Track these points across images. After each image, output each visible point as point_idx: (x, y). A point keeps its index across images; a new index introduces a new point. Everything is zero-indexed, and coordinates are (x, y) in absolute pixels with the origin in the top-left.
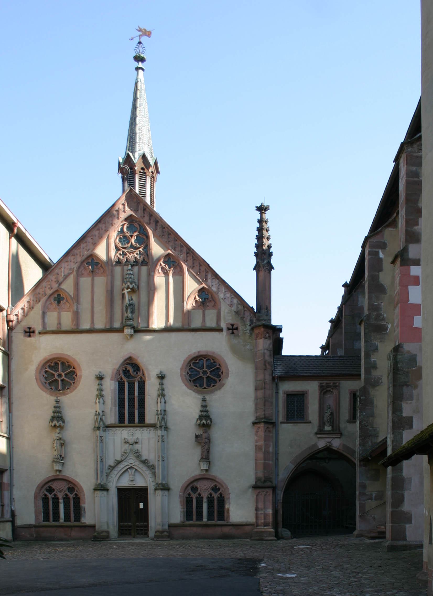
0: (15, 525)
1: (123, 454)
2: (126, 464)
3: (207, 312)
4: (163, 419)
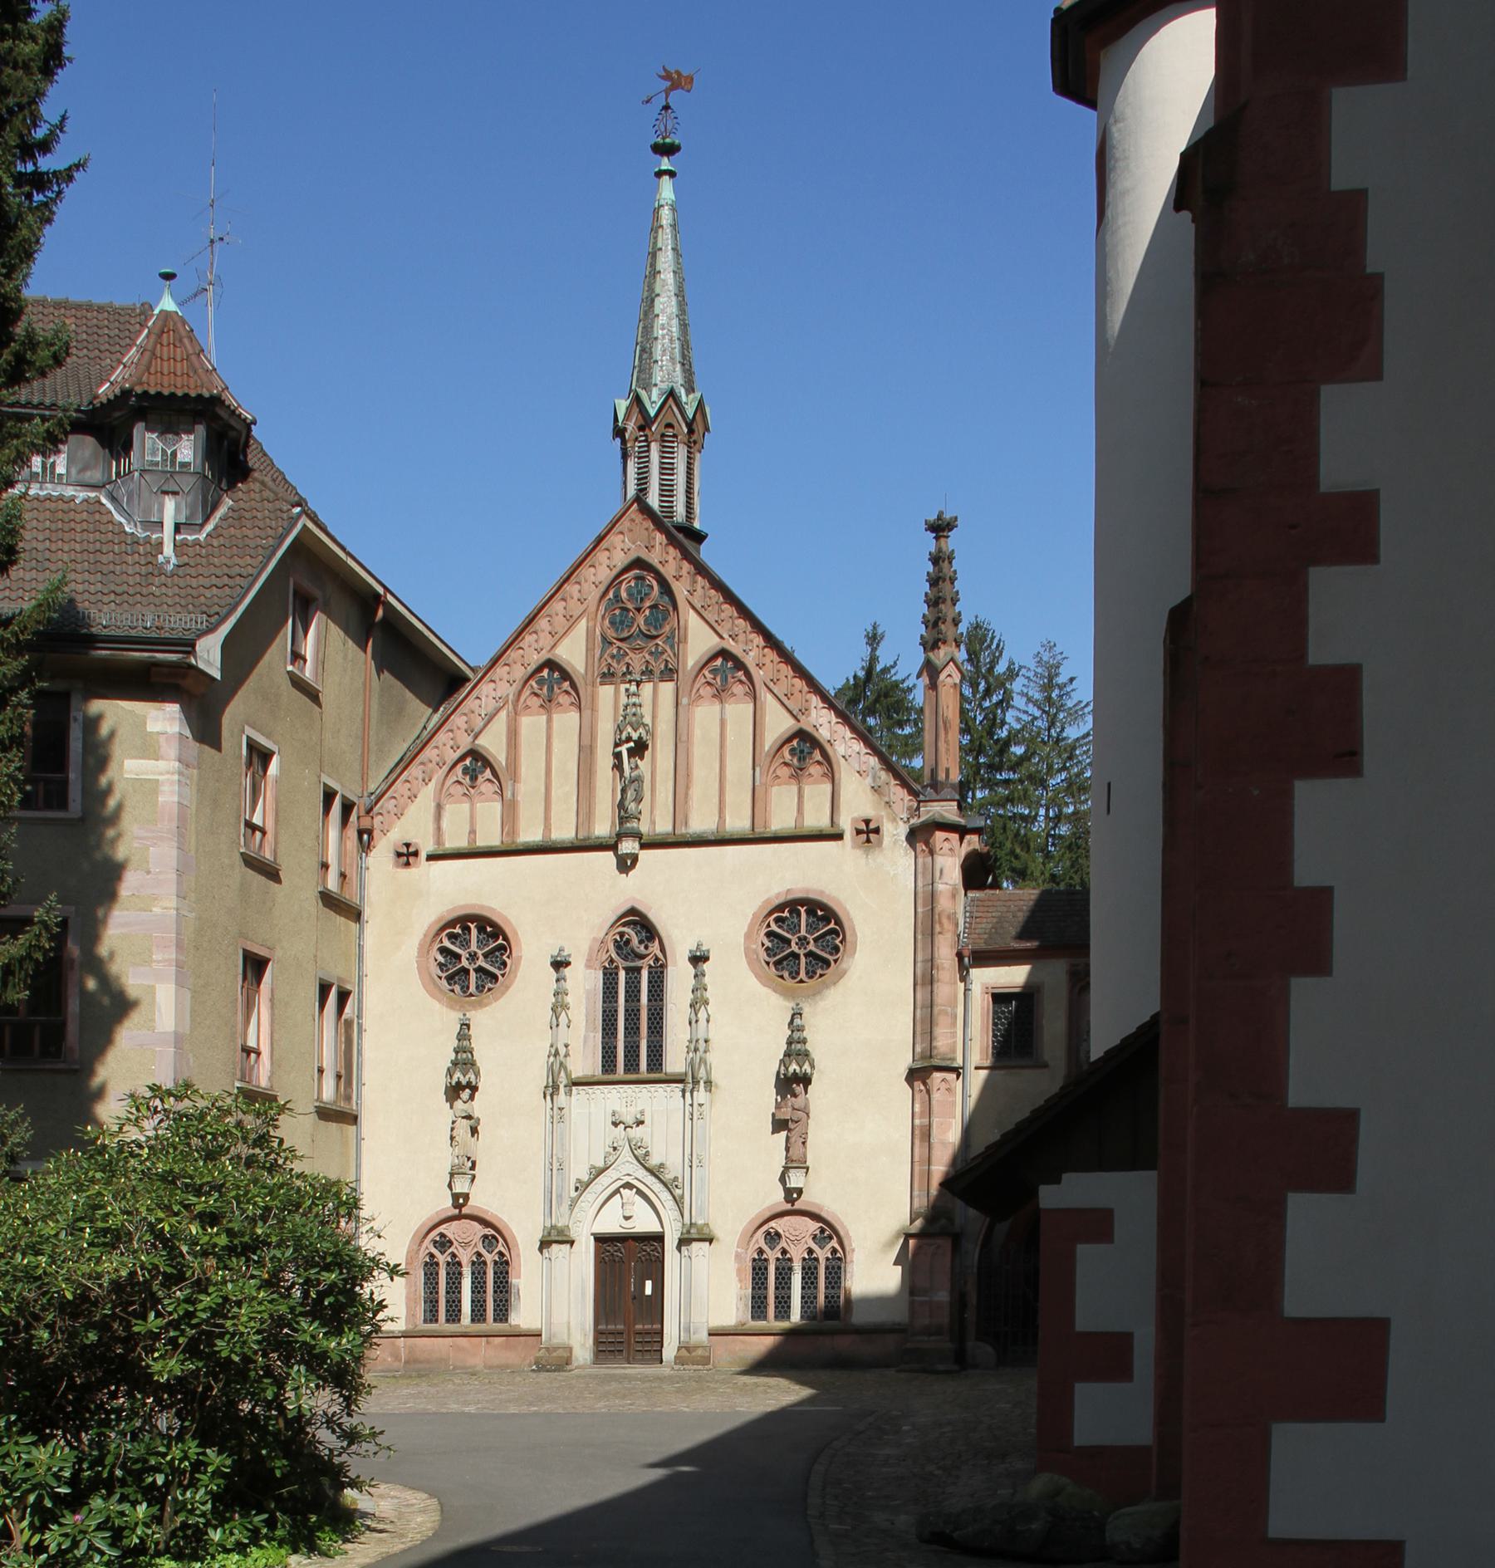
4: (703, 1061)
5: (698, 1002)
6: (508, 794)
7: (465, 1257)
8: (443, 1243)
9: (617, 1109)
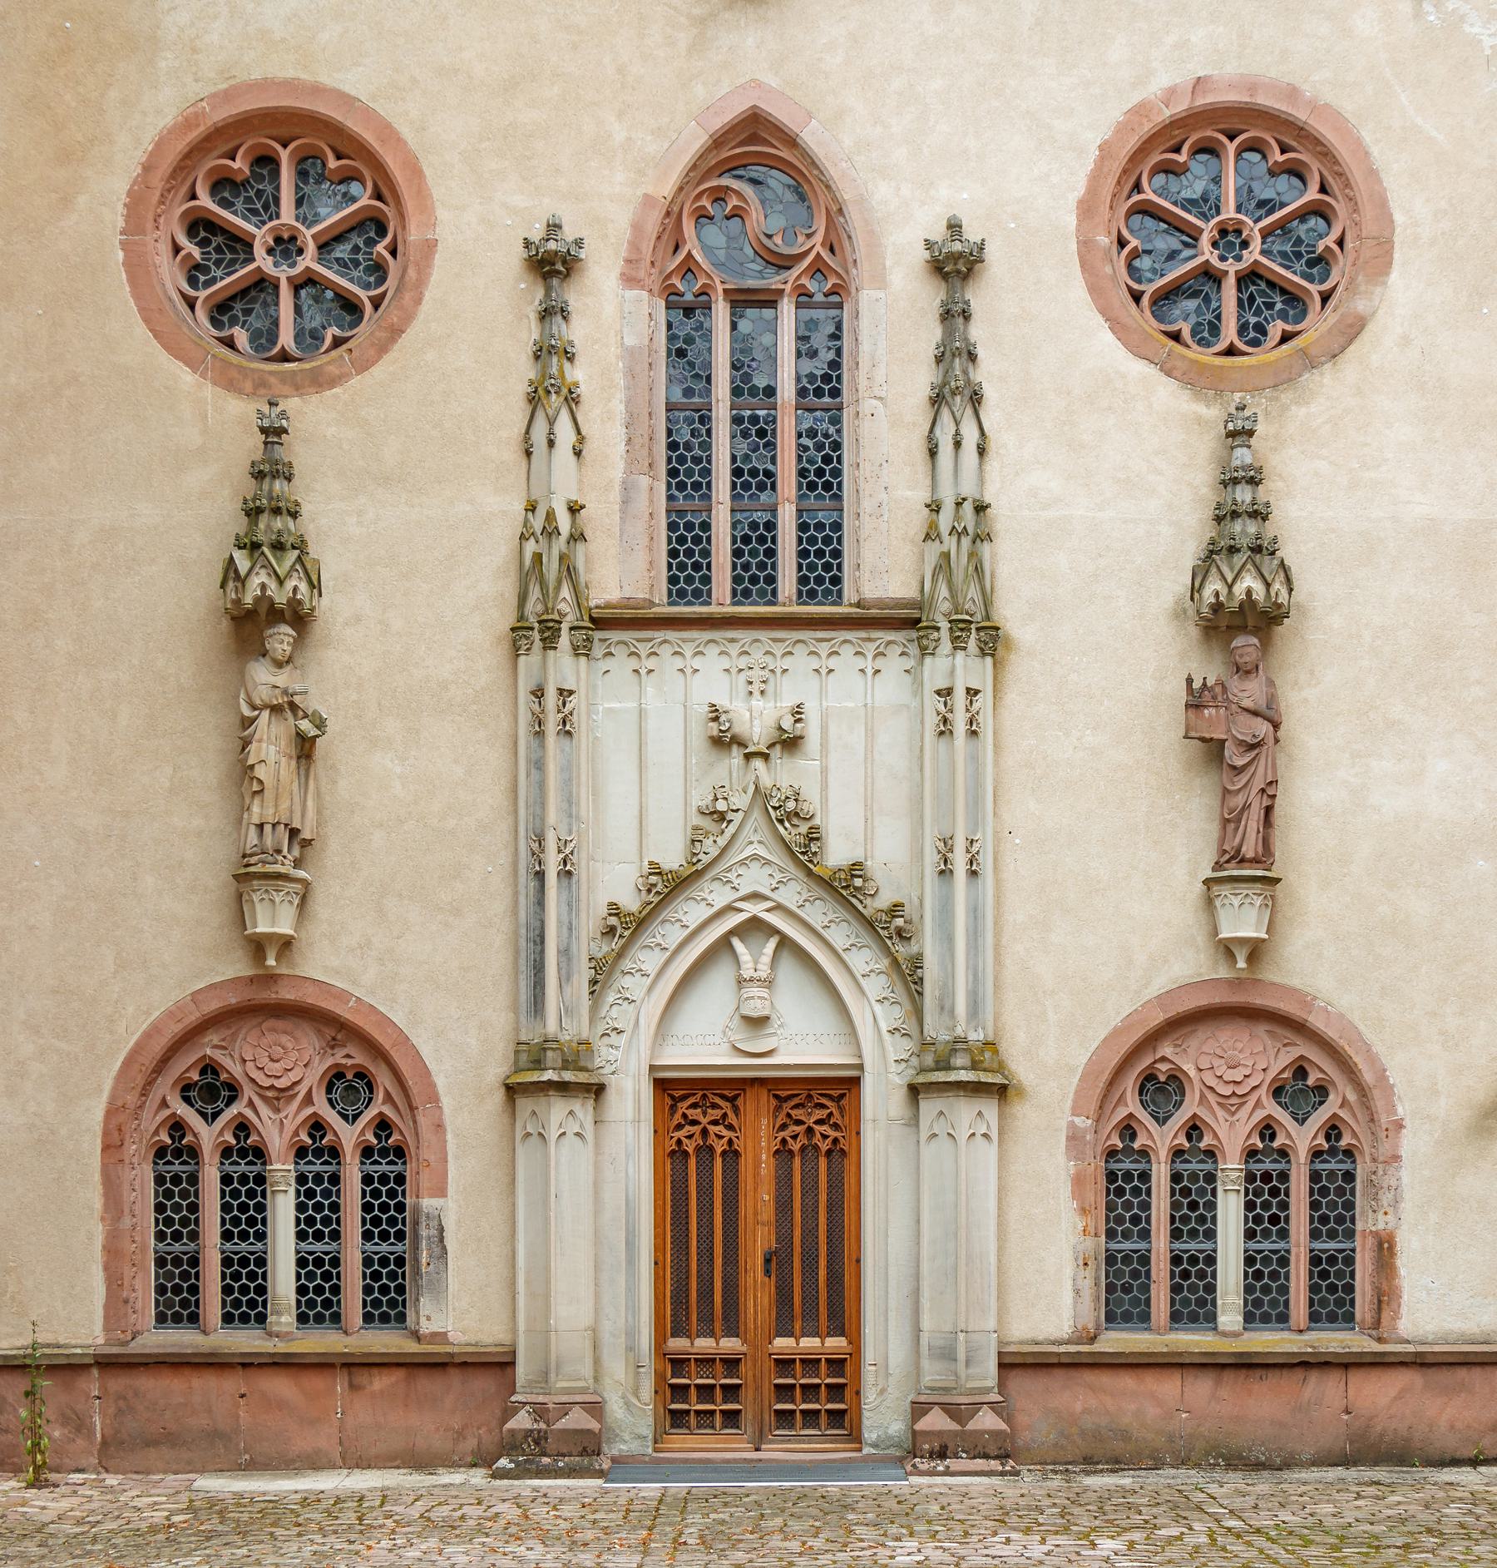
5: (955, 389)
7: (277, 1132)
8: (212, 1089)
9: (722, 702)
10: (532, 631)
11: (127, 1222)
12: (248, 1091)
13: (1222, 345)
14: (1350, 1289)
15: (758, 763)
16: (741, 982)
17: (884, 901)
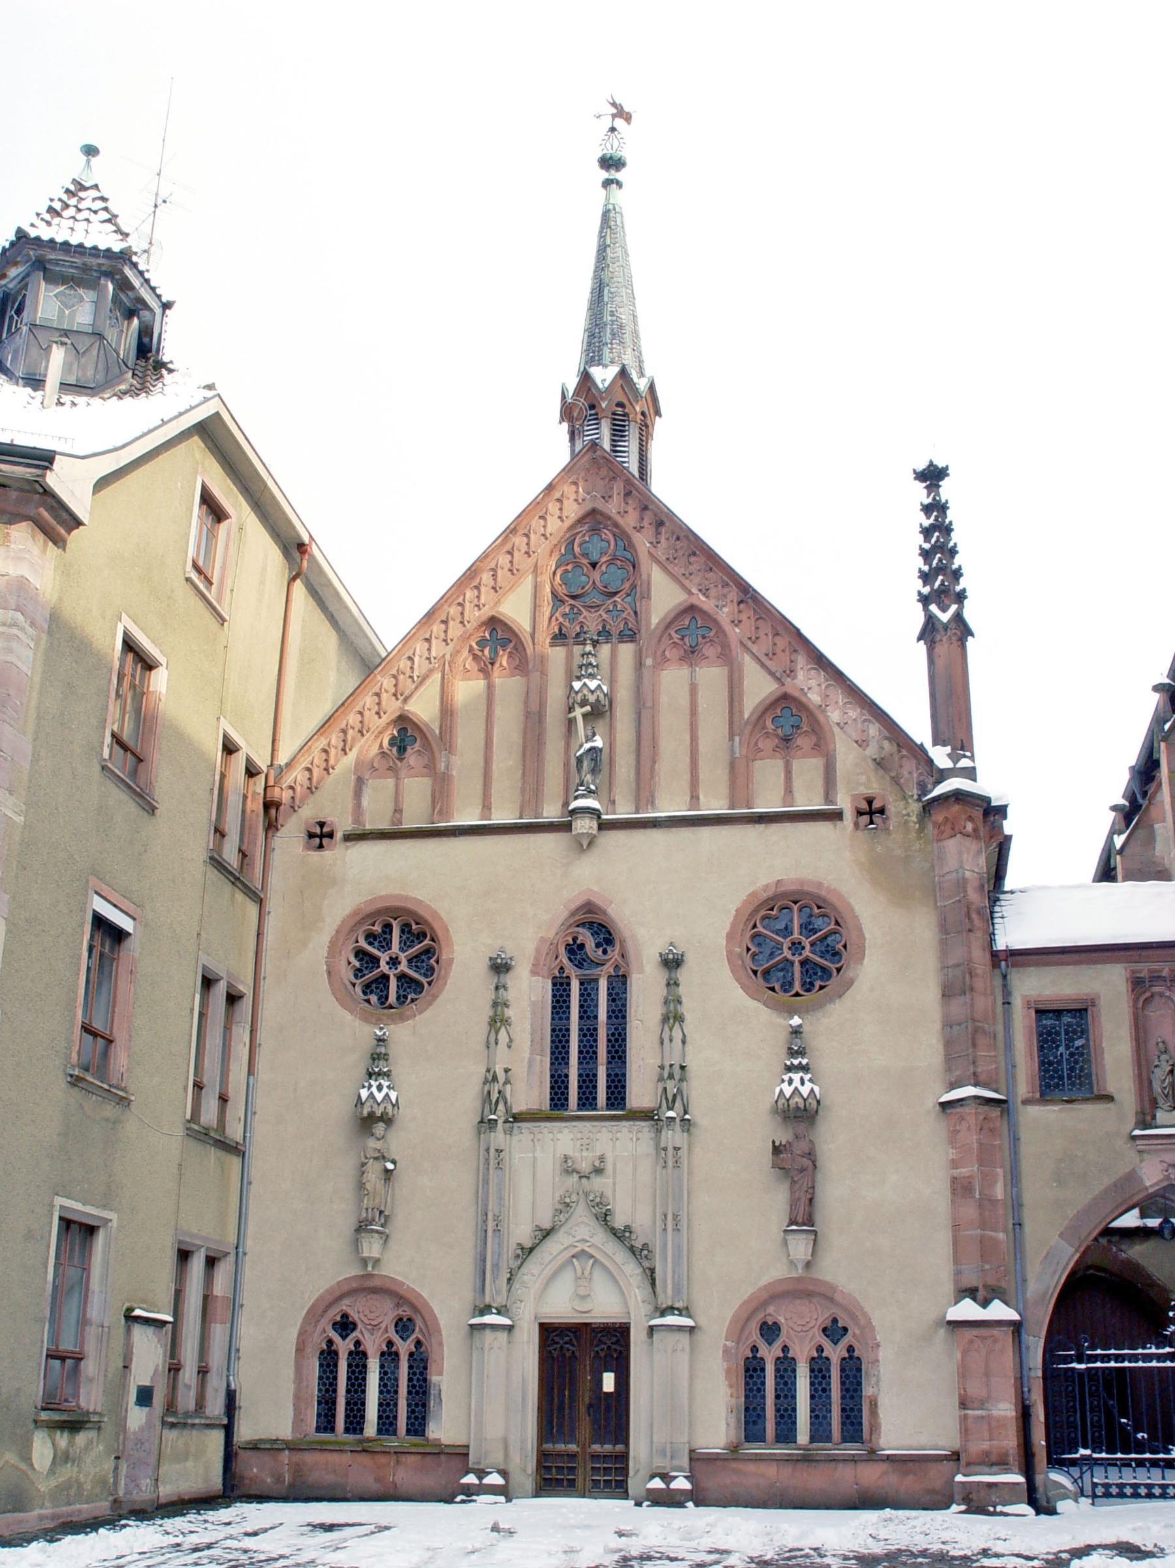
0: (235, 1439)
1: (560, 1207)
2: (571, 1240)
3: (796, 765)
5: (672, 1017)
6: (442, 767)
7: (373, 1346)
8: (345, 1326)
9: (570, 1153)
10: (486, 1124)
11: (304, 1384)
12: (360, 1326)
13: (793, 992)
14: (861, 1424)
15: (584, 1180)
16: (577, 1278)
17: (638, 1244)
